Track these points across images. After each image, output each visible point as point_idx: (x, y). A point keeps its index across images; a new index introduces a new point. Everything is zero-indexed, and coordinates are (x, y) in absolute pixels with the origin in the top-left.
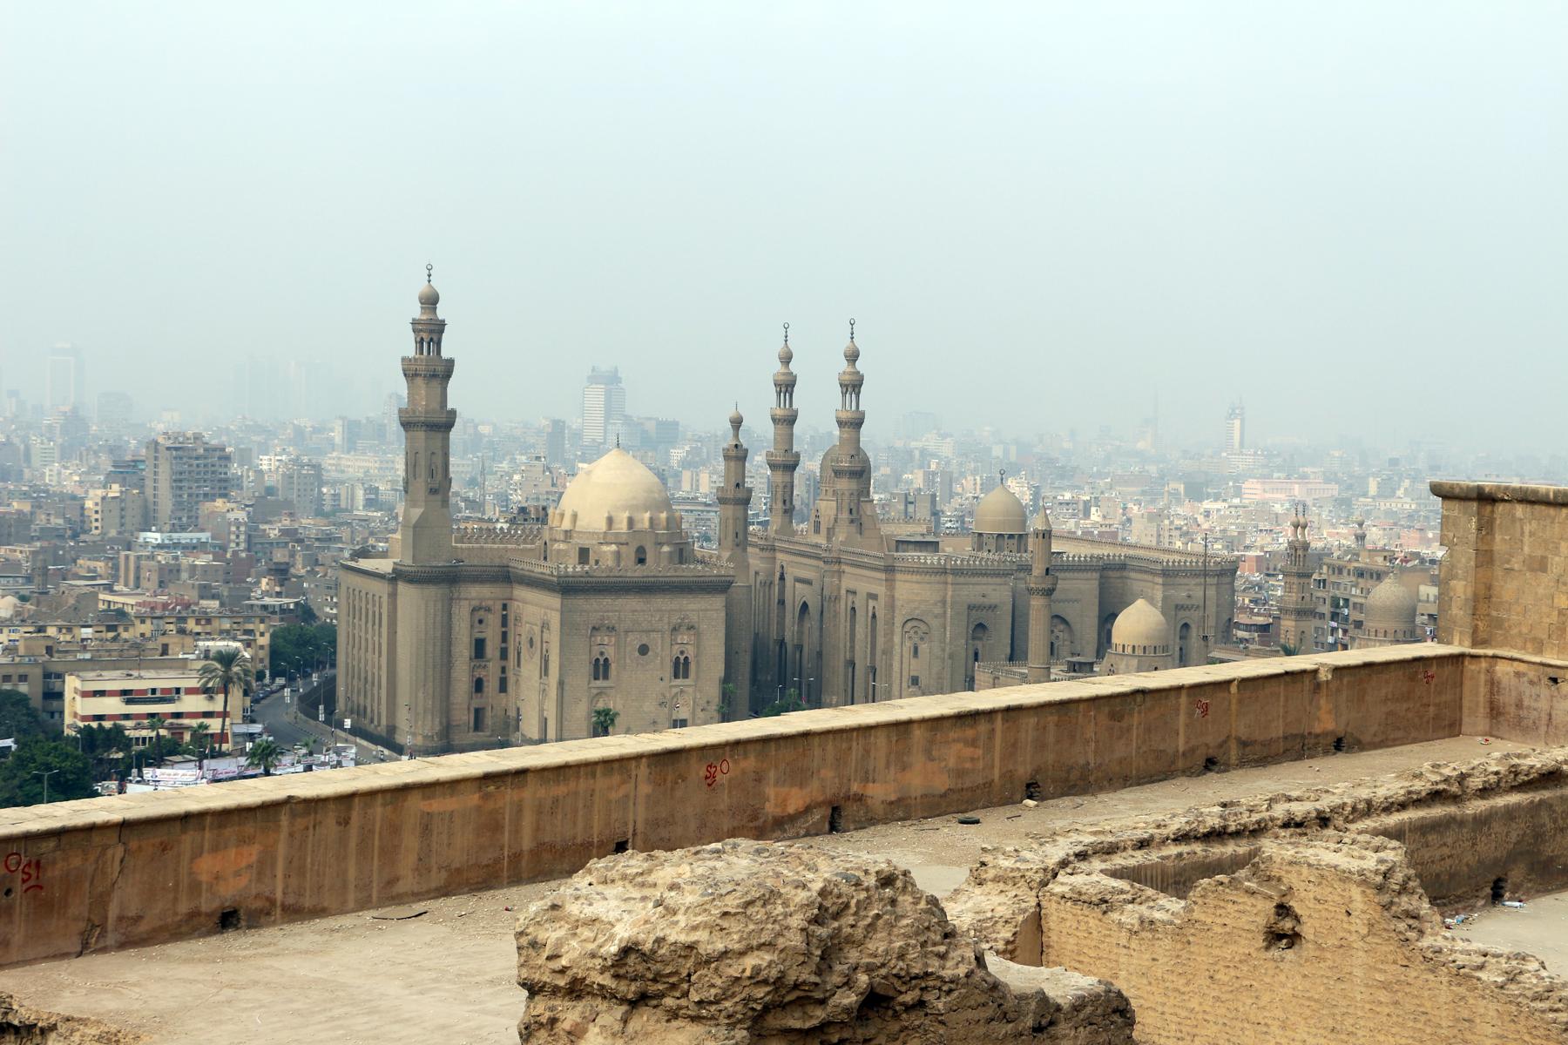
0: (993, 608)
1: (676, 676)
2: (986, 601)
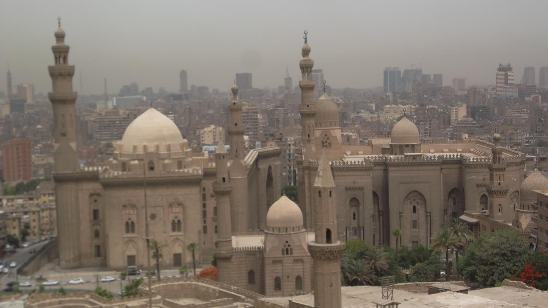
0: (361, 189)
2: (356, 185)
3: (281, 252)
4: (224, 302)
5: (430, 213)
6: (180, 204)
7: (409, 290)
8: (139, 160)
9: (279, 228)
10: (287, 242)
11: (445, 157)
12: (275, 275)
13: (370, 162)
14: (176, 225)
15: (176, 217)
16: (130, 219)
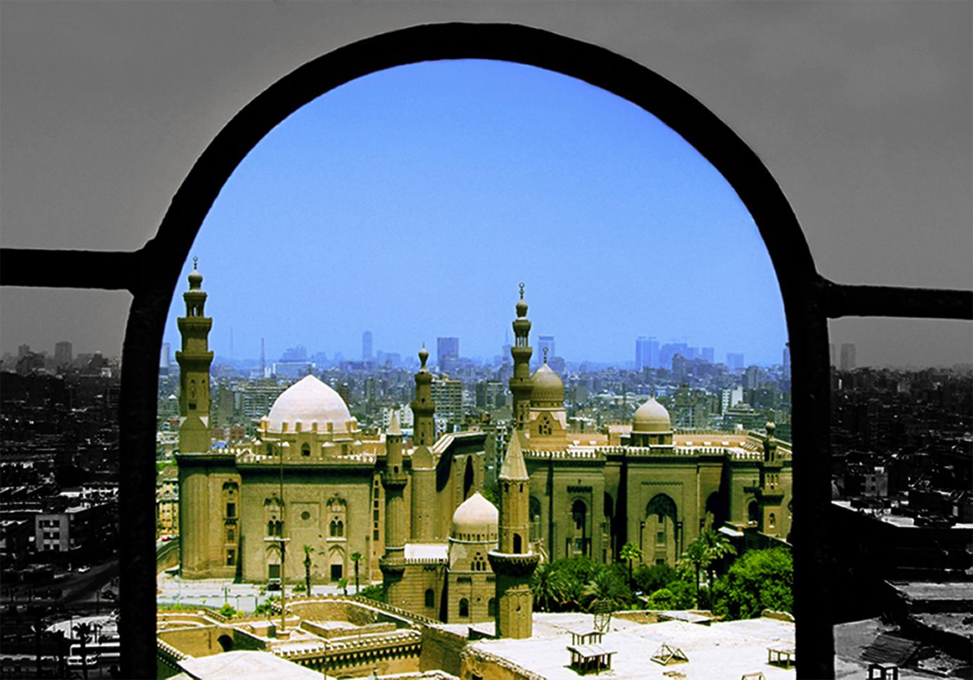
0: (589, 489)
1: (333, 534)
2: (583, 484)
3: (470, 567)
4: (383, 627)
5: (681, 523)
6: (343, 502)
7: (635, 620)
8: (290, 442)
9: (469, 536)
10: (478, 554)
11: (703, 451)
12: (460, 597)
13: (603, 454)
14: (336, 528)
15: (337, 518)
16: (274, 517)
